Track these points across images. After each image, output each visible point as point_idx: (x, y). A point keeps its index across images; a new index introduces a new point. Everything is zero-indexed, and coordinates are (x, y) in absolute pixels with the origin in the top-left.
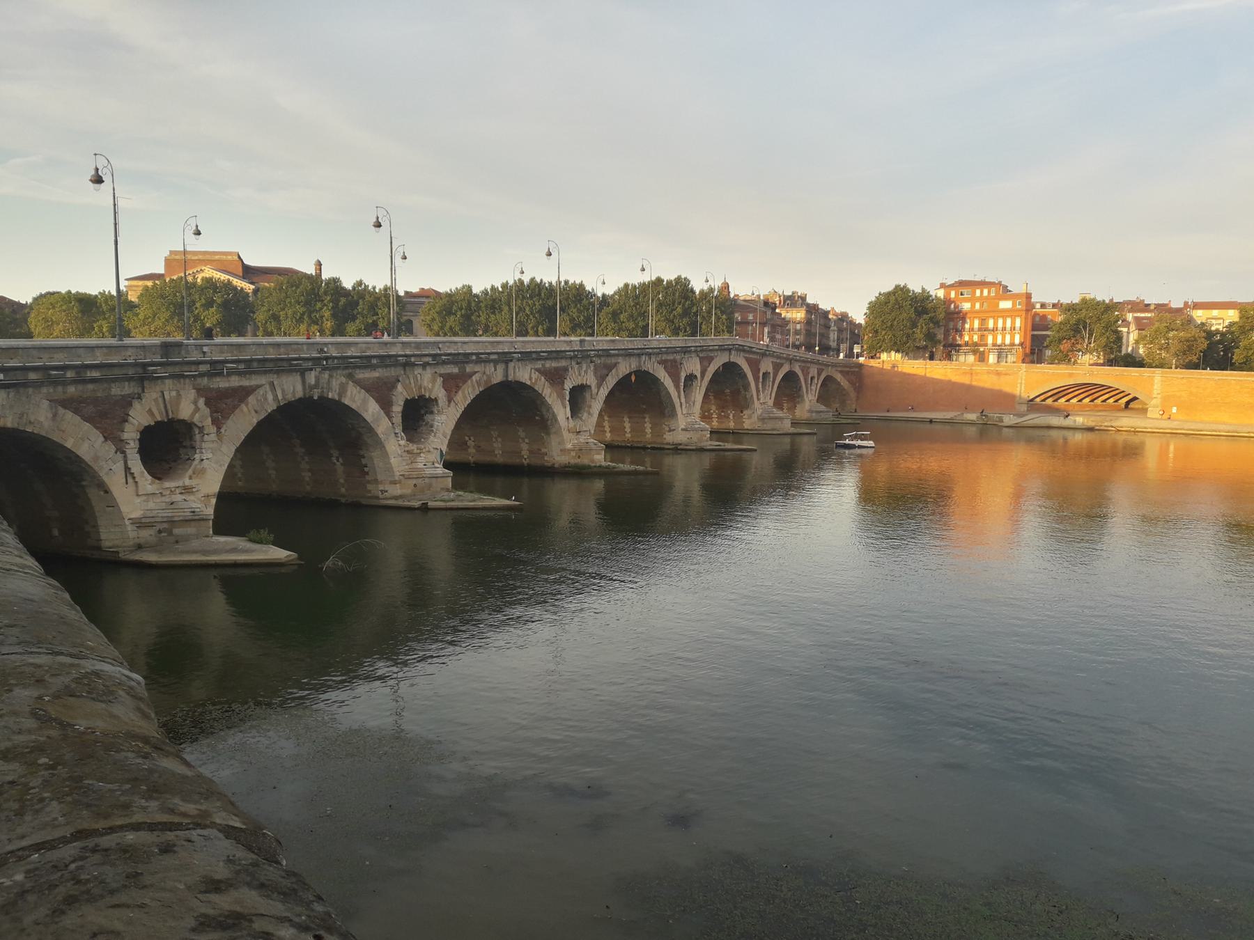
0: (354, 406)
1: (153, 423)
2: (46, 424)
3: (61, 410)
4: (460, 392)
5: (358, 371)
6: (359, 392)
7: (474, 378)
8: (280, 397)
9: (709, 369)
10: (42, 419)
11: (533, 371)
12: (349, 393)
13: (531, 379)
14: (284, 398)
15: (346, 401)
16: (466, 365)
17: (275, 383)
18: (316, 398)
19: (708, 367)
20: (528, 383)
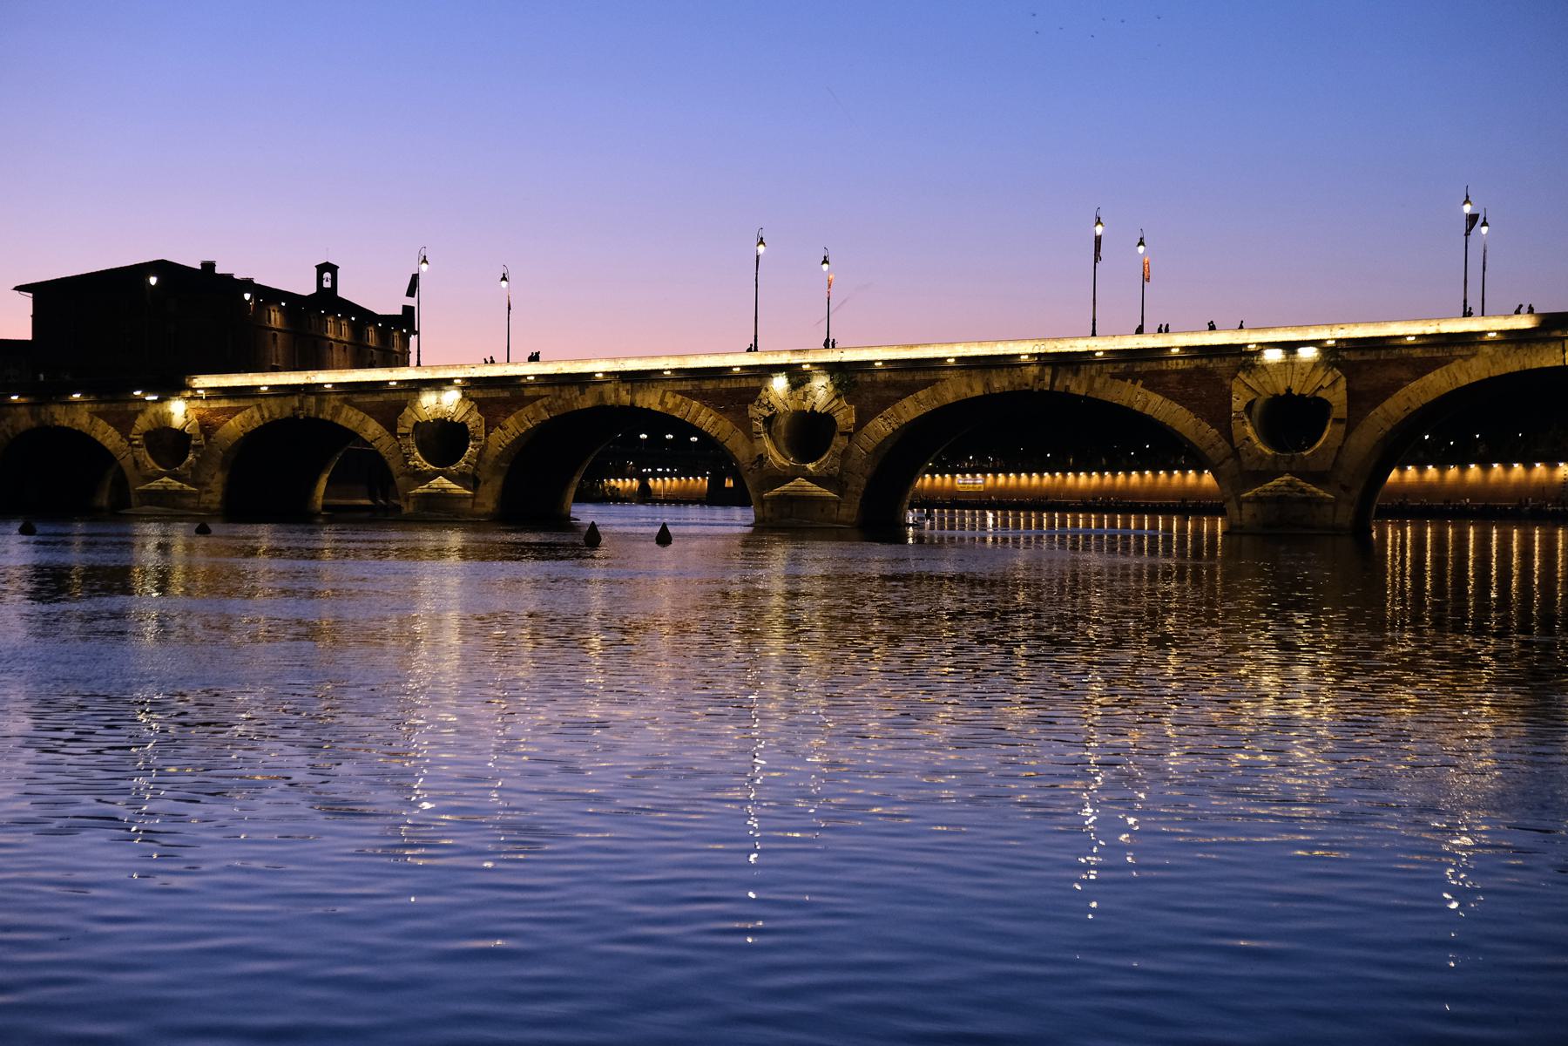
0: (350, 427)
1: (152, 429)
2: (86, 426)
3: (96, 418)
4: (512, 418)
5: (355, 396)
6: (356, 415)
7: (539, 403)
8: (266, 415)
9: (1412, 385)
10: (84, 422)
11: (668, 394)
12: (343, 415)
13: (662, 402)
14: (270, 417)
15: (341, 421)
16: (522, 389)
17: (263, 405)
18: (302, 417)
19: (1411, 380)
20: (659, 408)
